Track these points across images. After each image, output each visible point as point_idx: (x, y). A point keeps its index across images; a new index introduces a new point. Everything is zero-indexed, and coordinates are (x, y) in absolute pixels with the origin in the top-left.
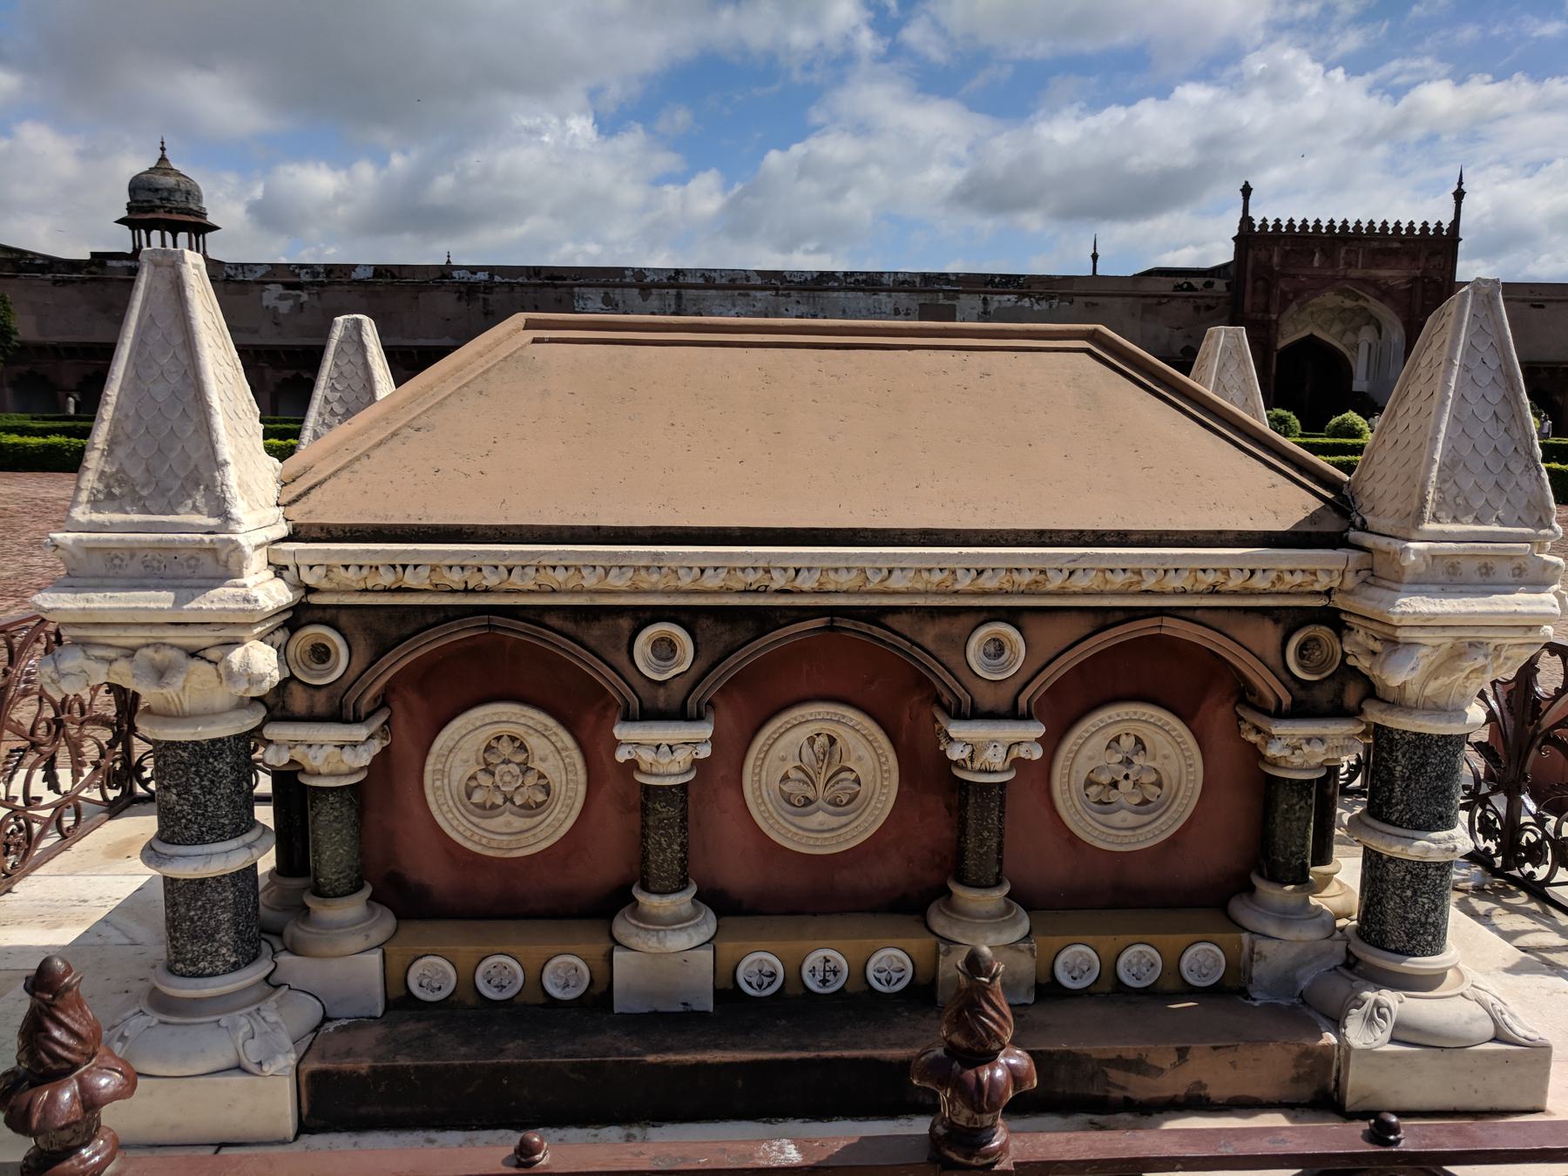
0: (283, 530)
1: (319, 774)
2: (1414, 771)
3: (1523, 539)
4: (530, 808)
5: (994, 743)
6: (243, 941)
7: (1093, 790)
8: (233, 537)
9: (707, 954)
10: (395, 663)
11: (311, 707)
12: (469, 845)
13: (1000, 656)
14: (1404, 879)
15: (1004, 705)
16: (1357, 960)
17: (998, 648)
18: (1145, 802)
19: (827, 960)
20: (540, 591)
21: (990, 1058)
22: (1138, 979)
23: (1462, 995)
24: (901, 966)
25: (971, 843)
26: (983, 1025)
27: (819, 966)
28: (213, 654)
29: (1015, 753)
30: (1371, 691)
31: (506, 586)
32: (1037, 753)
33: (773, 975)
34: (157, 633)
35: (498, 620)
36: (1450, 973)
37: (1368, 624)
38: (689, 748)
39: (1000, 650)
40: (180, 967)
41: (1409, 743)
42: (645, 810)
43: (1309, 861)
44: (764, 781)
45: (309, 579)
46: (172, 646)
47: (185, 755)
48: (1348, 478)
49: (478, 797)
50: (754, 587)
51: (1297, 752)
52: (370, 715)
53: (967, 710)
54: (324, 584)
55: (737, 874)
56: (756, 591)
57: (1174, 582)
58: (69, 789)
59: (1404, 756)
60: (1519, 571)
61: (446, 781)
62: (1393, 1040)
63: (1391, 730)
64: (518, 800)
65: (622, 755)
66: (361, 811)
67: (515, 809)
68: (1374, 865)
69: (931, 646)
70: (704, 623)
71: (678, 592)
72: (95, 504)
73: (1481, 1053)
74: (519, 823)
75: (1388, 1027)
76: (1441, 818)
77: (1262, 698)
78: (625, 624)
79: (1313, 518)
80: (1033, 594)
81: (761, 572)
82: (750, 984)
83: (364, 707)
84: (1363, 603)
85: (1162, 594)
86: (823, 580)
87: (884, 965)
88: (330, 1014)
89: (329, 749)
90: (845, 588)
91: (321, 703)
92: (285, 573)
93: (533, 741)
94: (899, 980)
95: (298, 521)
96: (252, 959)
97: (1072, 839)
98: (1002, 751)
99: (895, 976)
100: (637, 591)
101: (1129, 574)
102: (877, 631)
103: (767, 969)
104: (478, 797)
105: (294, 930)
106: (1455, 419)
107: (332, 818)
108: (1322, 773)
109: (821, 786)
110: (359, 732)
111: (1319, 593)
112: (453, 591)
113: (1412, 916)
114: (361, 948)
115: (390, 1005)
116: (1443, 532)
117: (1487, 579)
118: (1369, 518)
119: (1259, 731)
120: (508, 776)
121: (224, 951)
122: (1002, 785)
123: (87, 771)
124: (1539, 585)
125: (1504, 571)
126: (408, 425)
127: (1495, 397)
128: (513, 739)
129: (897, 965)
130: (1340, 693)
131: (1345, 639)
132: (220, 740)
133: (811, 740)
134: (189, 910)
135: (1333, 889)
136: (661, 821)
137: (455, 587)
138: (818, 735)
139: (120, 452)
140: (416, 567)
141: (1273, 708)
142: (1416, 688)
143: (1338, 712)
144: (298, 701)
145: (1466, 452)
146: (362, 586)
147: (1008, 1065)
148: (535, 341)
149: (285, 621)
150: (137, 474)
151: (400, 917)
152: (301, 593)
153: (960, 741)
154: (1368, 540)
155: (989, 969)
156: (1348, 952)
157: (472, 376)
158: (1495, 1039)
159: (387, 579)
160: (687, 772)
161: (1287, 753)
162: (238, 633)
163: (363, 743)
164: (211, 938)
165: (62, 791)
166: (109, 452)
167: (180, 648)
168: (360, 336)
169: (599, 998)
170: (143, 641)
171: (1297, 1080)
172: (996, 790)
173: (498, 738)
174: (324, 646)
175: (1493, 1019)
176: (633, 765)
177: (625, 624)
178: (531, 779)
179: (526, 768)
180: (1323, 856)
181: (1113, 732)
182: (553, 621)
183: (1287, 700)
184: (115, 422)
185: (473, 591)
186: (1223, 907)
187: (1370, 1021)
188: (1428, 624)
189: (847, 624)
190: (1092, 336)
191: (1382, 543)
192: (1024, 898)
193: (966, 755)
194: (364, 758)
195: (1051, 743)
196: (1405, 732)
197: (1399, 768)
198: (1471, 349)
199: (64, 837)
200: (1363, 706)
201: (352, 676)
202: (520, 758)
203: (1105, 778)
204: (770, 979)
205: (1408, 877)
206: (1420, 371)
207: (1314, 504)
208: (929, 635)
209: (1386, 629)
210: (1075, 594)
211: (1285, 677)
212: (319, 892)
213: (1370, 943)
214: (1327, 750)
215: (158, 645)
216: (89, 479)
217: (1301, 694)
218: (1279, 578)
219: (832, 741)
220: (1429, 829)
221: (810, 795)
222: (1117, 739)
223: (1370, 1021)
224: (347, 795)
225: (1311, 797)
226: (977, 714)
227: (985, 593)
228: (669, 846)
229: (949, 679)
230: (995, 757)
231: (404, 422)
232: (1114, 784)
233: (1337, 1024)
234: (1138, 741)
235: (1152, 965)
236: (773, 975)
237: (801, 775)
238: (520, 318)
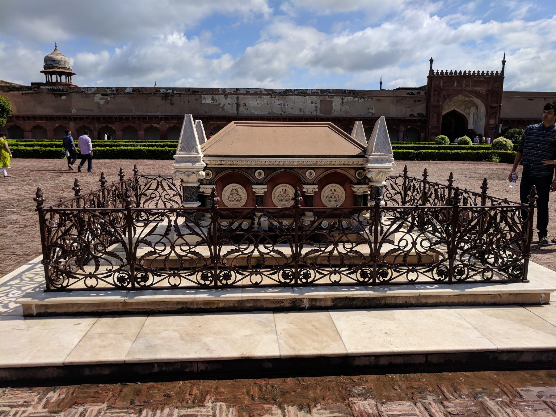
3: (387, 155)
4: (238, 201)
5: (310, 188)
7: (328, 198)
10: (219, 176)
15: (312, 183)
17: (311, 174)
20: (241, 165)
30: (370, 180)
35: (235, 169)
39: (311, 174)
45: (208, 163)
49: (230, 199)
53: (306, 183)
57: (337, 163)
60: (387, 160)
65: (254, 190)
69: (300, 173)
70: (266, 170)
71: (262, 165)
72: (180, 151)
74: (237, 203)
78: (254, 170)
79: (360, 153)
91: (208, 182)
93: (239, 190)
98: (312, 190)
100: (256, 165)
102: (292, 171)
104: (230, 199)
106: (377, 138)
117: (382, 161)
122: (312, 196)
124: (390, 162)
125: (385, 160)
127: (384, 134)
130: (365, 181)
133: (282, 190)
139: (183, 144)
143: (365, 184)
144: (205, 182)
145: (379, 143)
150: (185, 147)
159: (219, 163)
166: (181, 144)
171: (357, 239)
177: (254, 170)
178: (238, 196)
179: (237, 194)
181: (331, 188)
182: (243, 170)
183: (356, 182)
184: (182, 139)
188: (373, 168)
189: (288, 170)
190: (329, 124)
193: (306, 190)
198: (380, 127)
202: (237, 192)
203: (330, 196)
208: (300, 172)
215: (188, 172)
216: (179, 148)
219: (286, 190)
226: (308, 184)
229: (303, 178)
230: (310, 190)
232: (331, 197)
234: (335, 190)
238: (233, 122)
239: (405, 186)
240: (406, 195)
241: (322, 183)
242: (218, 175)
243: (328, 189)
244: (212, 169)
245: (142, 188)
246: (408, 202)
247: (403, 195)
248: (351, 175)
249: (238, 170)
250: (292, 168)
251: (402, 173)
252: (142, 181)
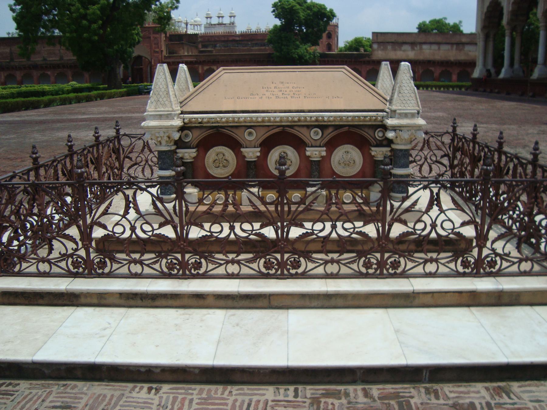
32: (324, 154)
182: (229, 128)
217: (378, 142)
239: (454, 145)
240: (454, 157)
245: (126, 149)
246: (457, 165)
247: (451, 159)
251: (450, 130)
252: (125, 142)
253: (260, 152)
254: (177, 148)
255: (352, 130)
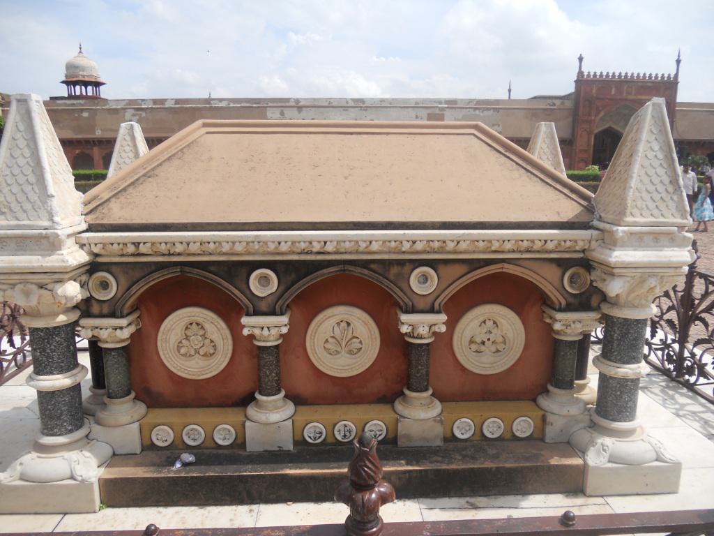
0: (84, 226)
1: (107, 342)
2: (622, 336)
6: (74, 419)
8: (56, 231)
9: (289, 423)
11: (101, 310)
12: (180, 374)
13: (426, 283)
14: (616, 387)
15: (428, 307)
16: (595, 424)
18: (498, 351)
19: (345, 426)
21: (370, 488)
22: (493, 434)
23: (643, 440)
24: (381, 428)
25: (413, 371)
26: (364, 470)
27: (342, 429)
28: (50, 287)
29: (433, 328)
30: (604, 298)
31: (187, 252)
32: (443, 329)
33: (321, 433)
34: (24, 277)
35: (187, 269)
36: (638, 429)
37: (602, 266)
38: (277, 329)
40: (48, 430)
41: (620, 323)
42: (259, 358)
43: (574, 378)
44: (316, 343)
45: (96, 250)
46: (32, 283)
47: (42, 334)
48: (594, 196)
49: (183, 351)
50: (306, 251)
51: (569, 328)
52: (128, 314)
54: (103, 252)
55: (304, 385)
56: (307, 253)
58: (19, 346)
59: (618, 329)
61: (168, 345)
62: (609, 461)
63: (612, 317)
64: (202, 352)
65: (246, 332)
66: (129, 360)
67: (200, 357)
68: (603, 378)
73: (650, 467)
75: (607, 455)
76: (634, 358)
77: (553, 302)
80: (441, 253)
81: (307, 244)
82: (310, 437)
83: (125, 312)
84: (598, 254)
85: (503, 252)
86: (338, 247)
87: (372, 428)
88: (117, 453)
89: (110, 330)
90: (350, 251)
91: (106, 310)
92: (85, 248)
93: (207, 326)
94: (380, 435)
95: (91, 223)
96: (79, 427)
97: (463, 369)
99: (378, 433)
101: (485, 242)
102: (366, 272)
103: (318, 430)
104: (183, 351)
105: (102, 415)
107: (113, 362)
108: (580, 337)
109: (343, 345)
110: (123, 322)
111: (579, 251)
112: (164, 255)
113: (619, 404)
114: (129, 422)
115: (144, 449)
116: (636, 222)
118: (602, 215)
119: (551, 318)
120: (196, 341)
121: (65, 424)
122: (428, 344)
123: (28, 338)
126: (144, 175)
128: (198, 324)
129: (380, 428)
130: (589, 299)
131: (592, 273)
132: (58, 327)
133: (338, 324)
134: (48, 405)
135: (587, 391)
136: (266, 363)
137: (164, 253)
138: (342, 321)
140: (144, 243)
141: (557, 307)
142: (624, 296)
146: (121, 253)
147: (379, 491)
148: (207, 133)
149: (87, 270)
151: (148, 407)
152: (92, 257)
153: (407, 323)
154: (601, 225)
155: (368, 444)
156: (591, 420)
157: (176, 151)
158: (656, 460)
160: (278, 340)
161: (564, 328)
162: (61, 276)
163: (126, 327)
164: (59, 418)
165: (16, 346)
167: (35, 284)
168: (133, 132)
169: (240, 443)
170: (18, 281)
172: (424, 347)
173: (191, 324)
174: (106, 282)
175: (656, 451)
176: (252, 337)
178: (207, 341)
180: (581, 374)
182: (212, 268)
183: (564, 303)
185: (173, 254)
186: (534, 400)
187: (598, 453)
188: (627, 266)
189: (352, 268)
190: (476, 127)
191: (607, 226)
192: (440, 396)
194: (126, 334)
195: (452, 324)
196: (619, 318)
197: (616, 335)
199: (19, 368)
200: (601, 305)
201: (119, 295)
203: (478, 340)
204: (319, 435)
205: (618, 386)
206: (627, 143)
207: (580, 209)
209: (610, 270)
210: (461, 253)
211: (563, 292)
212: (110, 397)
213: (601, 417)
214: (583, 326)
217: (571, 300)
218: (559, 244)
219: (348, 324)
220: (628, 363)
221: (339, 349)
222: (484, 322)
223: (598, 453)
224: (121, 351)
225: (575, 349)
226: (413, 310)
227: (417, 252)
228: (271, 374)
231: (141, 174)
232: (483, 343)
233: (583, 452)
234: (495, 323)
235: (499, 427)
236: (321, 433)
237: (334, 340)
238: (200, 122)
241: (457, 306)
242: (134, 289)
243: (474, 322)
244: (114, 269)
248: (546, 280)
249: (196, 270)
250: (365, 264)
253: (291, 323)
254: (81, 317)
255: (510, 269)
